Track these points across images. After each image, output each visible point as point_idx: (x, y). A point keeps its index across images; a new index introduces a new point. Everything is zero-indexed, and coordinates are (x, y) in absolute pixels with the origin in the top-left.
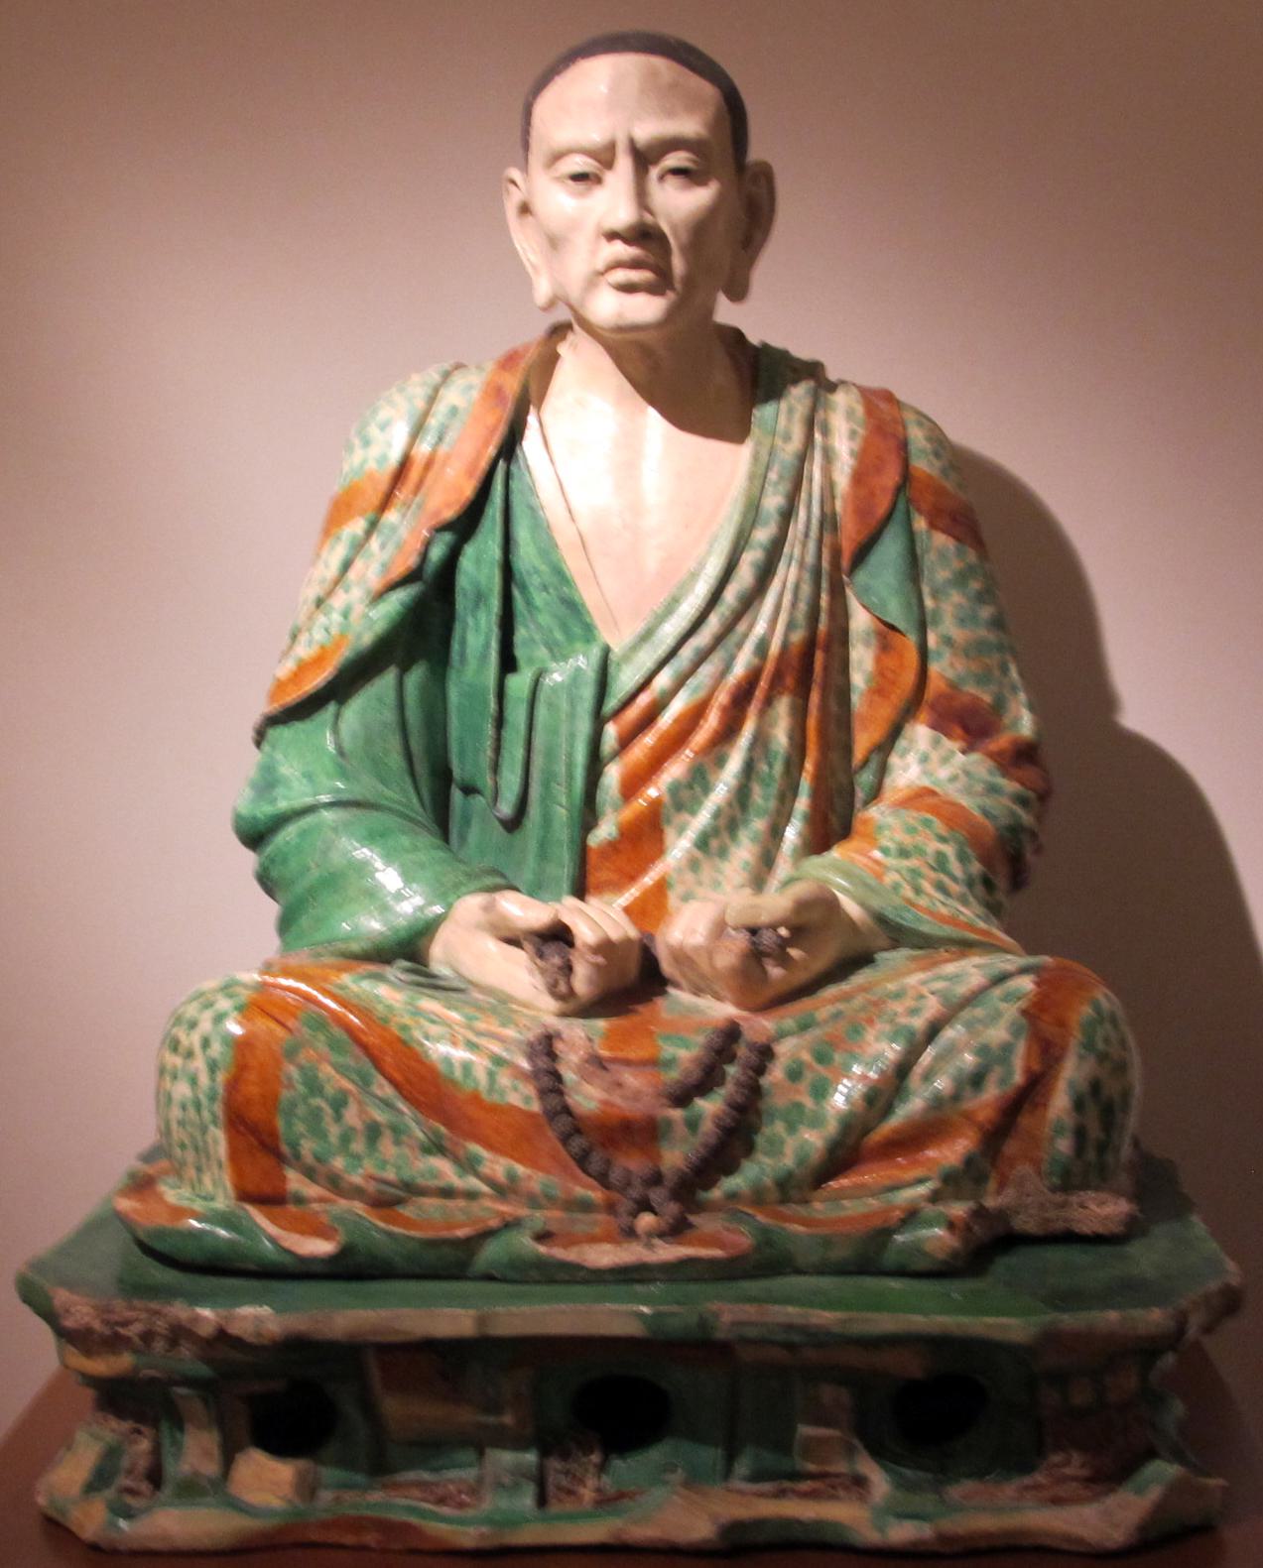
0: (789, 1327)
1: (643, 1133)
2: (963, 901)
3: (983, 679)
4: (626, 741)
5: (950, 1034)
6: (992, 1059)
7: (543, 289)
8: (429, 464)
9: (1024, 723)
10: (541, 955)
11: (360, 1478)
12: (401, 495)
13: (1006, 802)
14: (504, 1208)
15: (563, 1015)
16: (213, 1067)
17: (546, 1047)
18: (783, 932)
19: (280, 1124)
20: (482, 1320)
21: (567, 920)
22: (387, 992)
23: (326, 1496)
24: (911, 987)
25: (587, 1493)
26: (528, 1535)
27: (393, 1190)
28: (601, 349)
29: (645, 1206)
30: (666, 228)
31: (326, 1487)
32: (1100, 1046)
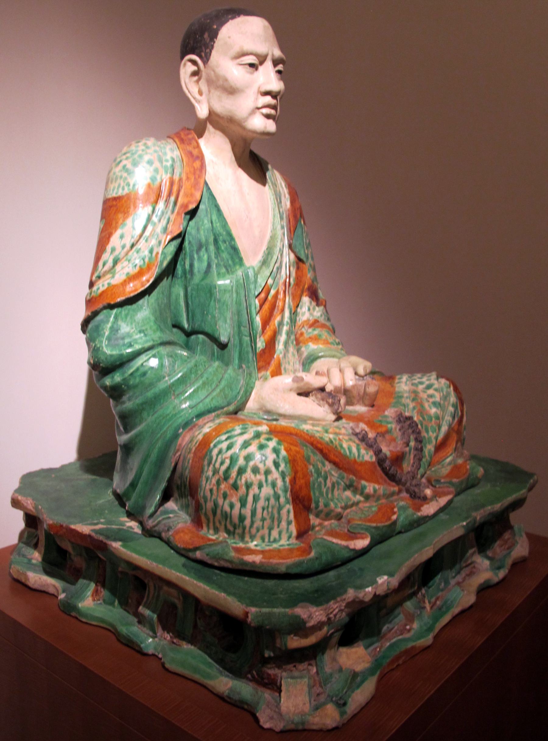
28: (228, 141)
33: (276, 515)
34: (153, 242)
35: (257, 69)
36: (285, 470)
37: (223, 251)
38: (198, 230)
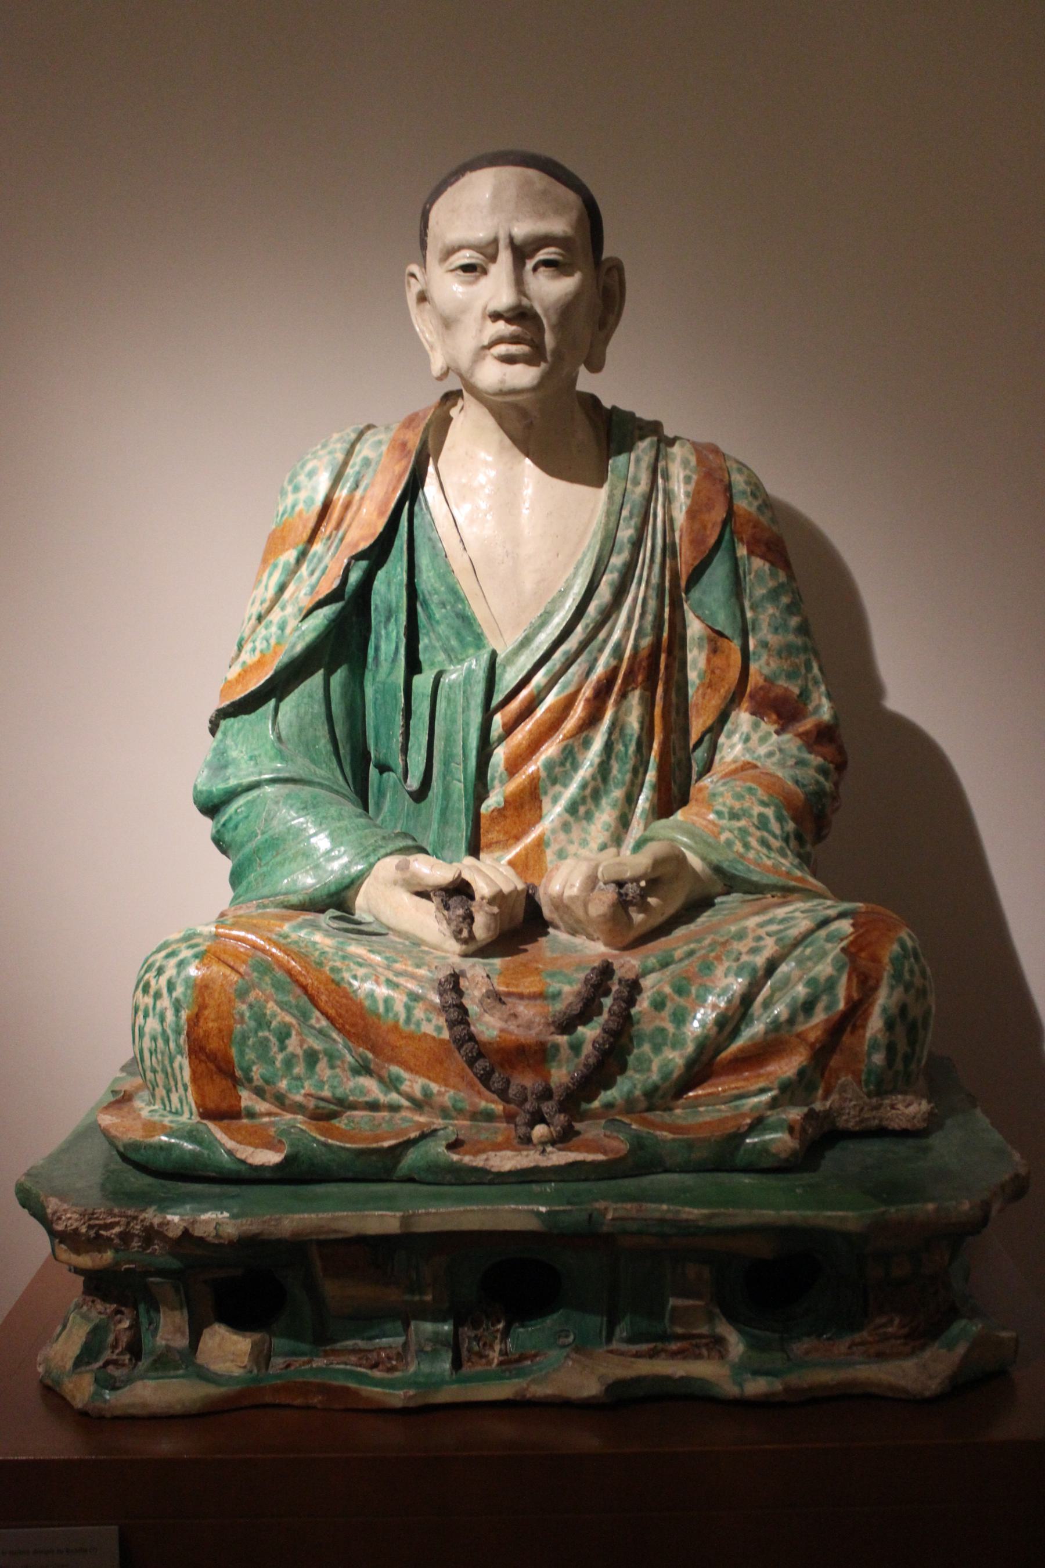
0: (662, 1221)
1: (537, 1055)
2: (784, 855)
3: (791, 676)
4: (510, 729)
5: (784, 968)
6: (821, 989)
7: (437, 364)
8: (347, 506)
9: (825, 711)
10: (447, 907)
11: (305, 1347)
12: (326, 530)
13: (812, 772)
14: (422, 1119)
15: (465, 955)
16: (177, 1006)
17: (453, 984)
18: (643, 884)
19: (234, 1052)
20: (405, 1220)
21: (467, 876)
22: (319, 937)
23: (278, 1362)
24: (751, 930)
25: (495, 1355)
26: (444, 1396)
27: (332, 1107)
28: (487, 411)
29: (538, 1118)
30: (539, 310)
31: (279, 1355)
32: (907, 976)
33: (169, 1070)
34: (290, 610)
35: (485, 272)
36: (181, 997)
37: (438, 622)
38: (389, 585)
